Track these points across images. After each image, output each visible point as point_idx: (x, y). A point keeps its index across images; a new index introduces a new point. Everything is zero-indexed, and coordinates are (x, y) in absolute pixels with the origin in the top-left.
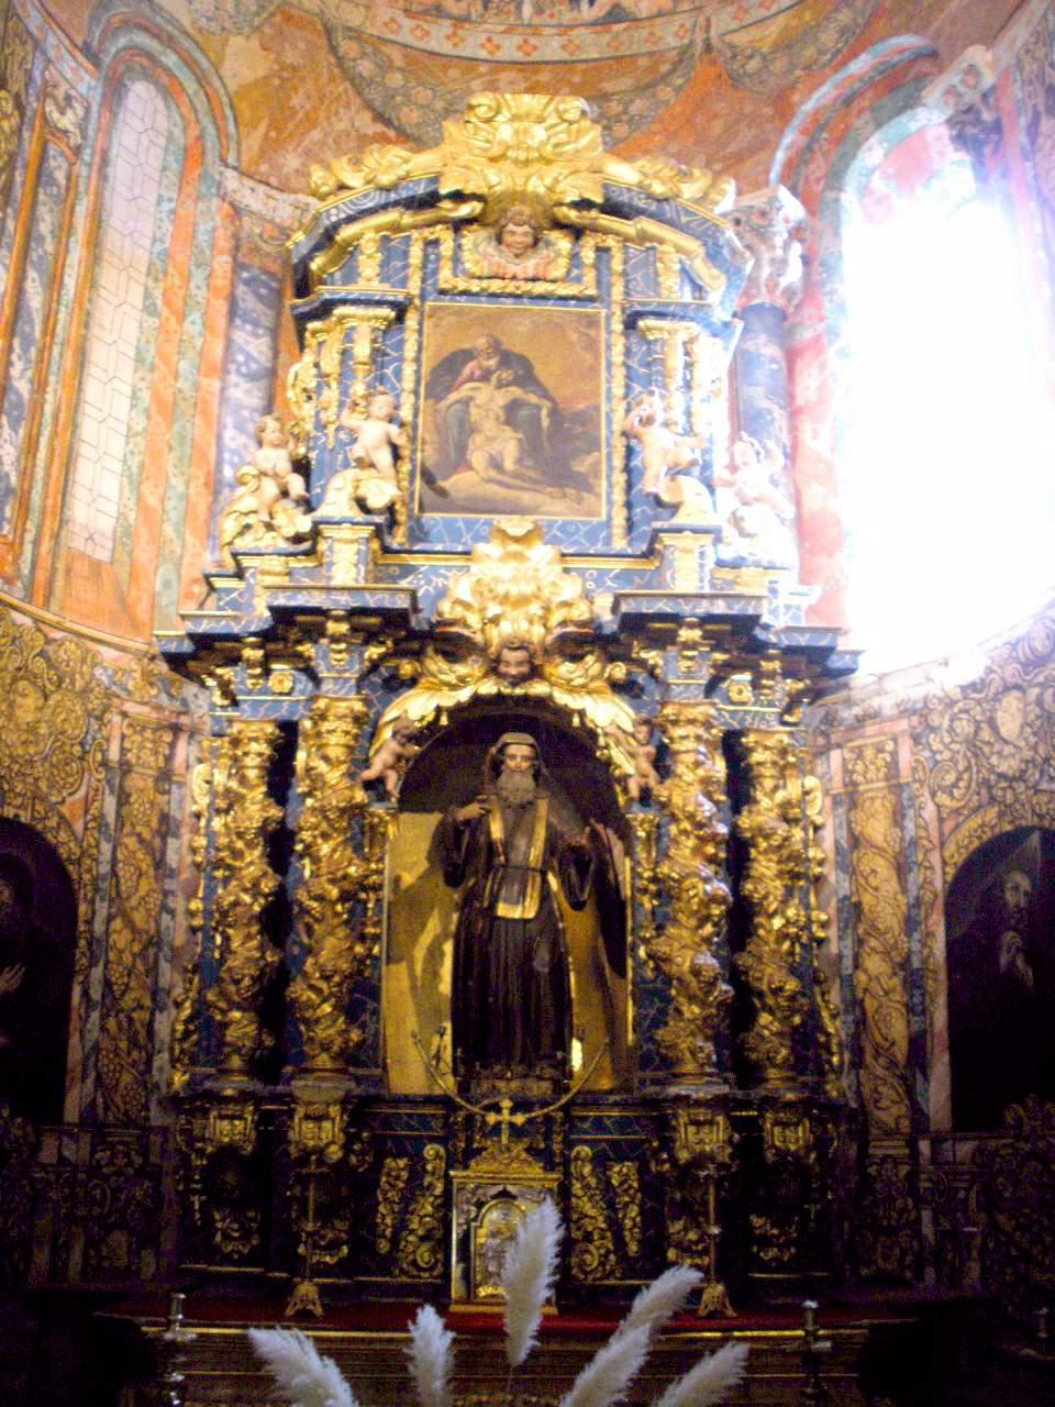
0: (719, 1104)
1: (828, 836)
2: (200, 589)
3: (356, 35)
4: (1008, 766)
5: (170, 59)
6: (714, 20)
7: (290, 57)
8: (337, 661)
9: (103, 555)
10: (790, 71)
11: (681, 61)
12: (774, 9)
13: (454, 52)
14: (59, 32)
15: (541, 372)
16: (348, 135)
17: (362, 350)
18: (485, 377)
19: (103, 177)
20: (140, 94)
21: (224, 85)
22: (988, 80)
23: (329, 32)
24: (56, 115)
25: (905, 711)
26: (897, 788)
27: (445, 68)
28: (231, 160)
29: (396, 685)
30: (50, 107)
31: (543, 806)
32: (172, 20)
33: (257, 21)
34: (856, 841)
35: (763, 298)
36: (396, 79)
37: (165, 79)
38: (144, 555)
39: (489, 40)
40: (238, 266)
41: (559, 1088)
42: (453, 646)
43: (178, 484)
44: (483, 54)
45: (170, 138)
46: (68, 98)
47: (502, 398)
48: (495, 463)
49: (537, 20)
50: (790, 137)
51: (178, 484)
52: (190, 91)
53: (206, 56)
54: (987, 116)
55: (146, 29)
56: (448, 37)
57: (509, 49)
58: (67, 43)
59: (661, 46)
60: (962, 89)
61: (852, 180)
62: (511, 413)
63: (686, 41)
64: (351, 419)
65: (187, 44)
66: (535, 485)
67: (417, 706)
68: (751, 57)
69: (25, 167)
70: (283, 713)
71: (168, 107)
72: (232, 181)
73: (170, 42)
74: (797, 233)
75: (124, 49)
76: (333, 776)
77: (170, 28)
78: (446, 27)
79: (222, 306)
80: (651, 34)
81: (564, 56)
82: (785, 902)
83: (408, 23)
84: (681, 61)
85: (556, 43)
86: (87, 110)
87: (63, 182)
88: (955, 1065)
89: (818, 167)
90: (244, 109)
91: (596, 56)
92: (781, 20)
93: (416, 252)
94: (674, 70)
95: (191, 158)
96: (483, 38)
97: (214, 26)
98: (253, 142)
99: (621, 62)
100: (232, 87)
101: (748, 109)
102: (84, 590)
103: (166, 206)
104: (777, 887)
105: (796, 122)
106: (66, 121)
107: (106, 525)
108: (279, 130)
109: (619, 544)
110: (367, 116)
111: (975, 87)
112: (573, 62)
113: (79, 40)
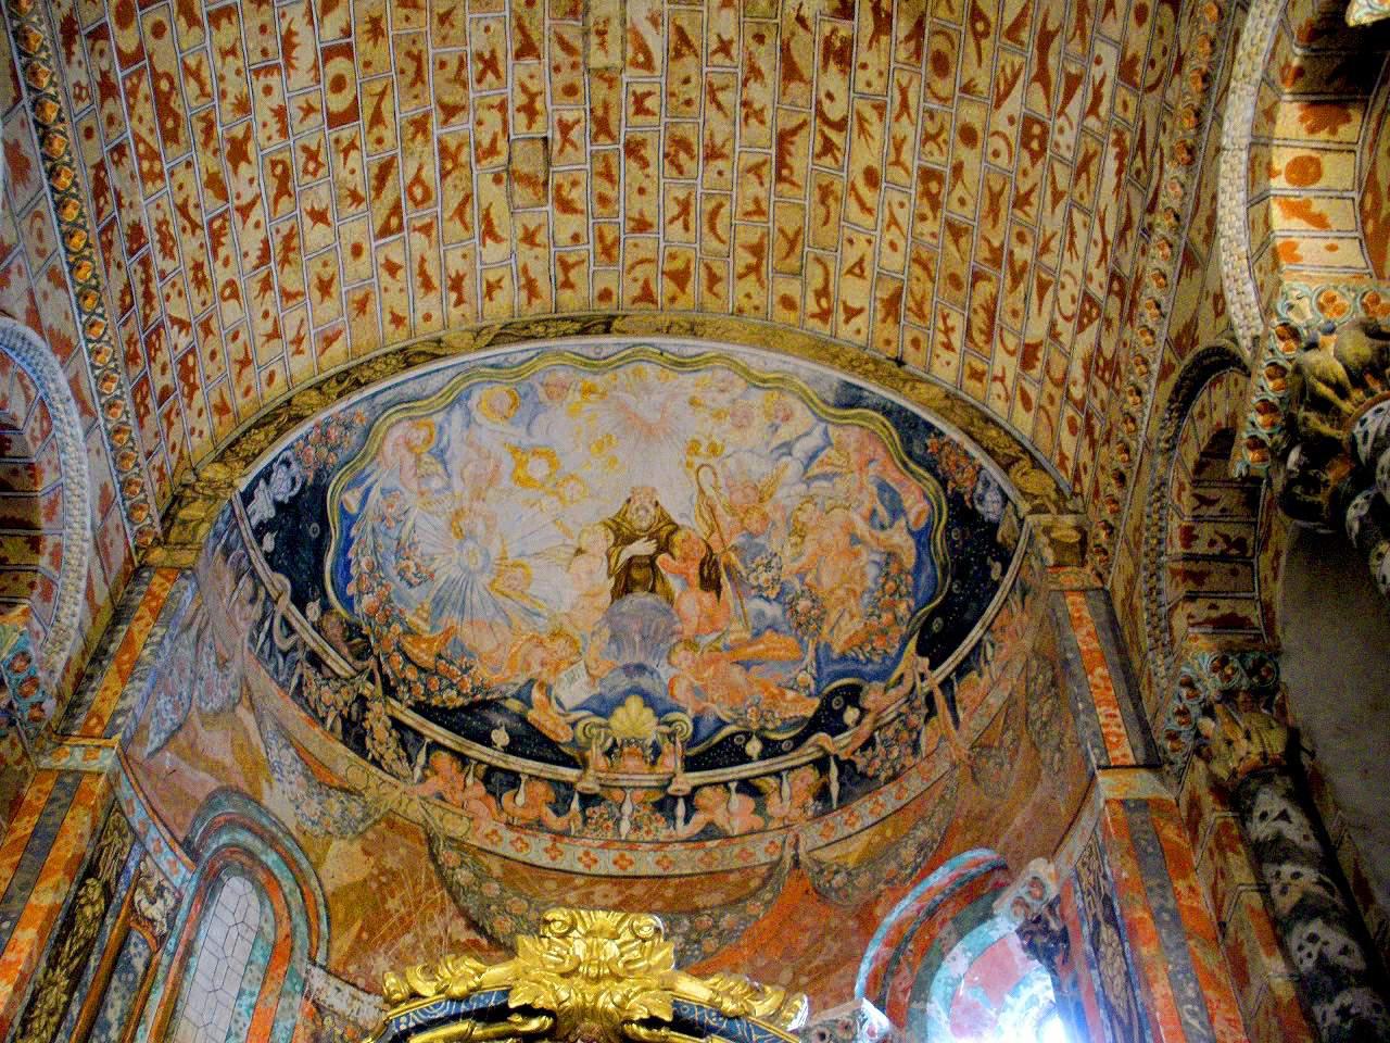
5: (271, 858)
6: (802, 838)
7: (390, 862)
11: (770, 876)
12: (858, 827)
13: (551, 864)
14: (161, 828)
16: (441, 941)
19: (184, 967)
20: (236, 892)
21: (321, 886)
22: (1052, 891)
23: (430, 840)
24: (145, 904)
27: (542, 879)
28: (320, 959)
30: (139, 896)
32: (277, 823)
33: (360, 829)
36: (493, 889)
37: (261, 876)
39: (587, 854)
44: (579, 867)
45: (260, 932)
46: (160, 889)
49: (633, 837)
50: (875, 949)
52: (286, 890)
53: (307, 857)
54: (1054, 926)
55: (250, 830)
56: (546, 850)
57: (606, 864)
58: (168, 836)
59: (751, 862)
60: (1028, 899)
61: (938, 989)
63: (775, 858)
65: (288, 843)
68: (836, 872)
69: (103, 953)
71: (261, 903)
72: (318, 979)
73: (272, 843)
75: (224, 845)
77: (274, 829)
78: (546, 840)
80: (743, 850)
81: (659, 871)
83: (509, 835)
84: (770, 876)
85: (651, 858)
86: (179, 901)
87: (140, 968)
89: (904, 979)
90: (340, 911)
91: (689, 871)
92: (864, 837)
94: (764, 884)
95: (280, 954)
96: (580, 852)
97: (318, 830)
98: (343, 943)
100: (329, 888)
101: (834, 922)
103: (247, 1000)
105: (880, 935)
106: (156, 911)
108: (372, 933)
110: (462, 922)
111: (1041, 898)
112: (667, 877)
113: (181, 836)
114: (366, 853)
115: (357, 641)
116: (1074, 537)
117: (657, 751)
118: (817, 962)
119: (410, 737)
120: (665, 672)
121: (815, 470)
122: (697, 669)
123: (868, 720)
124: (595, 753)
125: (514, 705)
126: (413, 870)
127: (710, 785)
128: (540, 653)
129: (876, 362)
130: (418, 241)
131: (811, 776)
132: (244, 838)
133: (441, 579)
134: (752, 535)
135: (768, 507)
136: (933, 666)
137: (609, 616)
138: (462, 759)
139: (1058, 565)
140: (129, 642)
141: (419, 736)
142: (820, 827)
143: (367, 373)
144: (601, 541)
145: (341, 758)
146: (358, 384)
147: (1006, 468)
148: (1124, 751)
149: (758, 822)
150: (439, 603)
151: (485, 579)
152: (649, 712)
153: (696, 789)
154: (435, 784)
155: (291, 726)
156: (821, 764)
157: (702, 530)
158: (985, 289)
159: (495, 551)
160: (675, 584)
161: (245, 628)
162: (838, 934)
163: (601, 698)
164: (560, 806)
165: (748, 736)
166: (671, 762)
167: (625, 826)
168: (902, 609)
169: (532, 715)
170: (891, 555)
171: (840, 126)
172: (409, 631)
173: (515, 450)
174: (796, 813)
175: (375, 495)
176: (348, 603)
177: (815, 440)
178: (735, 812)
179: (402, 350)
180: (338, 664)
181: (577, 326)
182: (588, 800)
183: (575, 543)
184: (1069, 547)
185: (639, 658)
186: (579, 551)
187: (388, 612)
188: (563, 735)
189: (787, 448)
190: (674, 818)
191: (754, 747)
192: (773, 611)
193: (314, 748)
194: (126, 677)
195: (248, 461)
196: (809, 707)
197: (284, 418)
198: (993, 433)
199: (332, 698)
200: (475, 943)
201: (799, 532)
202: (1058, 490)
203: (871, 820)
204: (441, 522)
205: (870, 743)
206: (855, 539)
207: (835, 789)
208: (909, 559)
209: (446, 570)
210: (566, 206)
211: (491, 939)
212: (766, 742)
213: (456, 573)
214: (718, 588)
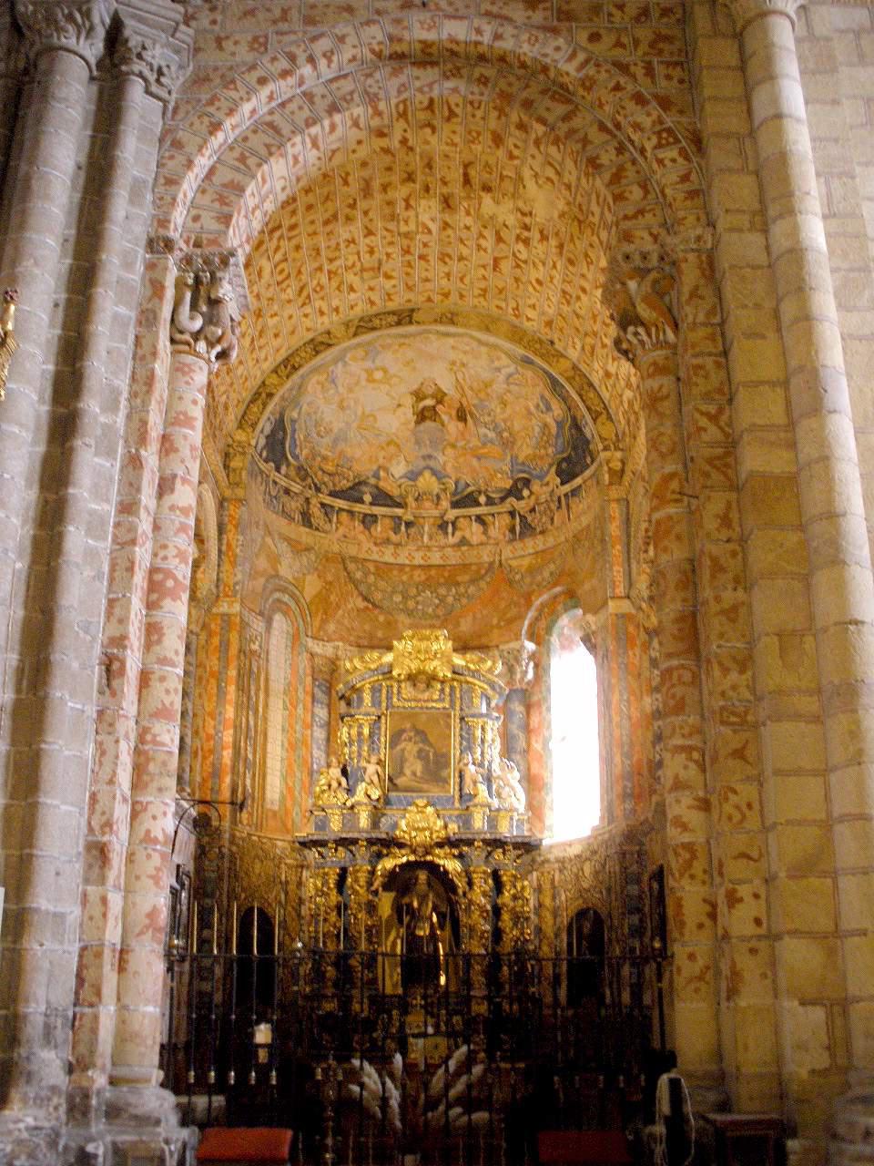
0: (483, 998)
1: (532, 903)
2: (308, 814)
3: (354, 559)
4: (585, 885)
5: (286, 598)
7: (330, 578)
8: (362, 852)
9: (276, 808)
10: (531, 584)
15: (431, 739)
17: (366, 731)
18: (410, 739)
20: (279, 620)
22: (594, 628)
25: (558, 860)
26: (554, 887)
27: (391, 570)
29: (379, 856)
31: (431, 896)
32: (286, 580)
34: (540, 905)
35: (518, 686)
36: (372, 579)
38: (289, 804)
40: (314, 679)
41: (436, 991)
42: (401, 846)
43: (298, 774)
44: (407, 562)
45: (288, 632)
47: (416, 749)
48: (414, 774)
50: (531, 614)
51: (298, 774)
57: (418, 561)
61: (556, 631)
62: (421, 755)
64: (363, 764)
65: (291, 587)
66: (427, 782)
67: (388, 864)
70: (342, 864)
72: (310, 642)
73: (284, 590)
74: (532, 656)
76: (361, 891)
79: (309, 699)
81: (442, 562)
82: (512, 930)
83: (375, 549)
85: (438, 555)
88: (568, 986)
89: (543, 624)
90: (313, 608)
93: (384, 691)
95: (295, 639)
98: (317, 623)
99: (465, 567)
102: (272, 823)
104: (511, 924)
105: (533, 608)
106: (255, 647)
107: (277, 797)
109: (457, 805)
110: (360, 599)
114: (319, 577)
115: (302, 473)
116: (617, 465)
117: (438, 497)
118: (509, 615)
119: (329, 510)
120: (441, 459)
121: (511, 380)
122: (456, 459)
123: (533, 498)
124: (410, 500)
125: (373, 481)
126: (339, 579)
127: (464, 517)
128: (382, 454)
129: (541, 341)
130: (318, 304)
131: (507, 519)
132: (277, 595)
133: (335, 431)
134: (481, 400)
135: (489, 390)
136: (563, 483)
137: (414, 433)
138: (351, 513)
139: (611, 484)
140: (229, 545)
141: (332, 507)
142: (510, 547)
143: (298, 359)
144: (409, 401)
145: (304, 535)
146: (295, 369)
147: (595, 420)
148: (620, 590)
149: (484, 538)
150: (336, 441)
151: (355, 425)
152: (434, 479)
153: (457, 518)
154: (341, 530)
155: (283, 531)
156: (512, 514)
157: (458, 396)
158: (589, 340)
159: (359, 413)
160: (445, 418)
161: (260, 498)
162: (517, 604)
163: (412, 472)
164: (396, 530)
165: (480, 492)
166: (445, 504)
167: (426, 538)
168: (550, 450)
169: (381, 484)
170: (546, 425)
171: (525, 262)
172: (325, 458)
173: (366, 371)
174: (501, 537)
175: (305, 407)
176: (296, 457)
177: (512, 369)
178: (474, 532)
179: (312, 340)
180: (296, 488)
181: (395, 318)
182: (409, 524)
183: (396, 402)
184: (615, 472)
185: (429, 451)
186: (399, 405)
187: (314, 454)
188: (395, 492)
189: (498, 370)
190: (447, 533)
191: (482, 499)
192: (491, 435)
193: (293, 536)
194: (234, 564)
195: (254, 426)
196: (508, 484)
197: (264, 395)
198: (591, 395)
199: (294, 505)
200: (367, 608)
201: (504, 404)
202: (617, 435)
203: (531, 551)
204: (334, 407)
205: (533, 510)
206: (530, 413)
207: (518, 528)
208: (554, 430)
209: (337, 426)
210: (388, 277)
211: (374, 604)
212: (488, 497)
213: (342, 425)
214: (465, 420)
